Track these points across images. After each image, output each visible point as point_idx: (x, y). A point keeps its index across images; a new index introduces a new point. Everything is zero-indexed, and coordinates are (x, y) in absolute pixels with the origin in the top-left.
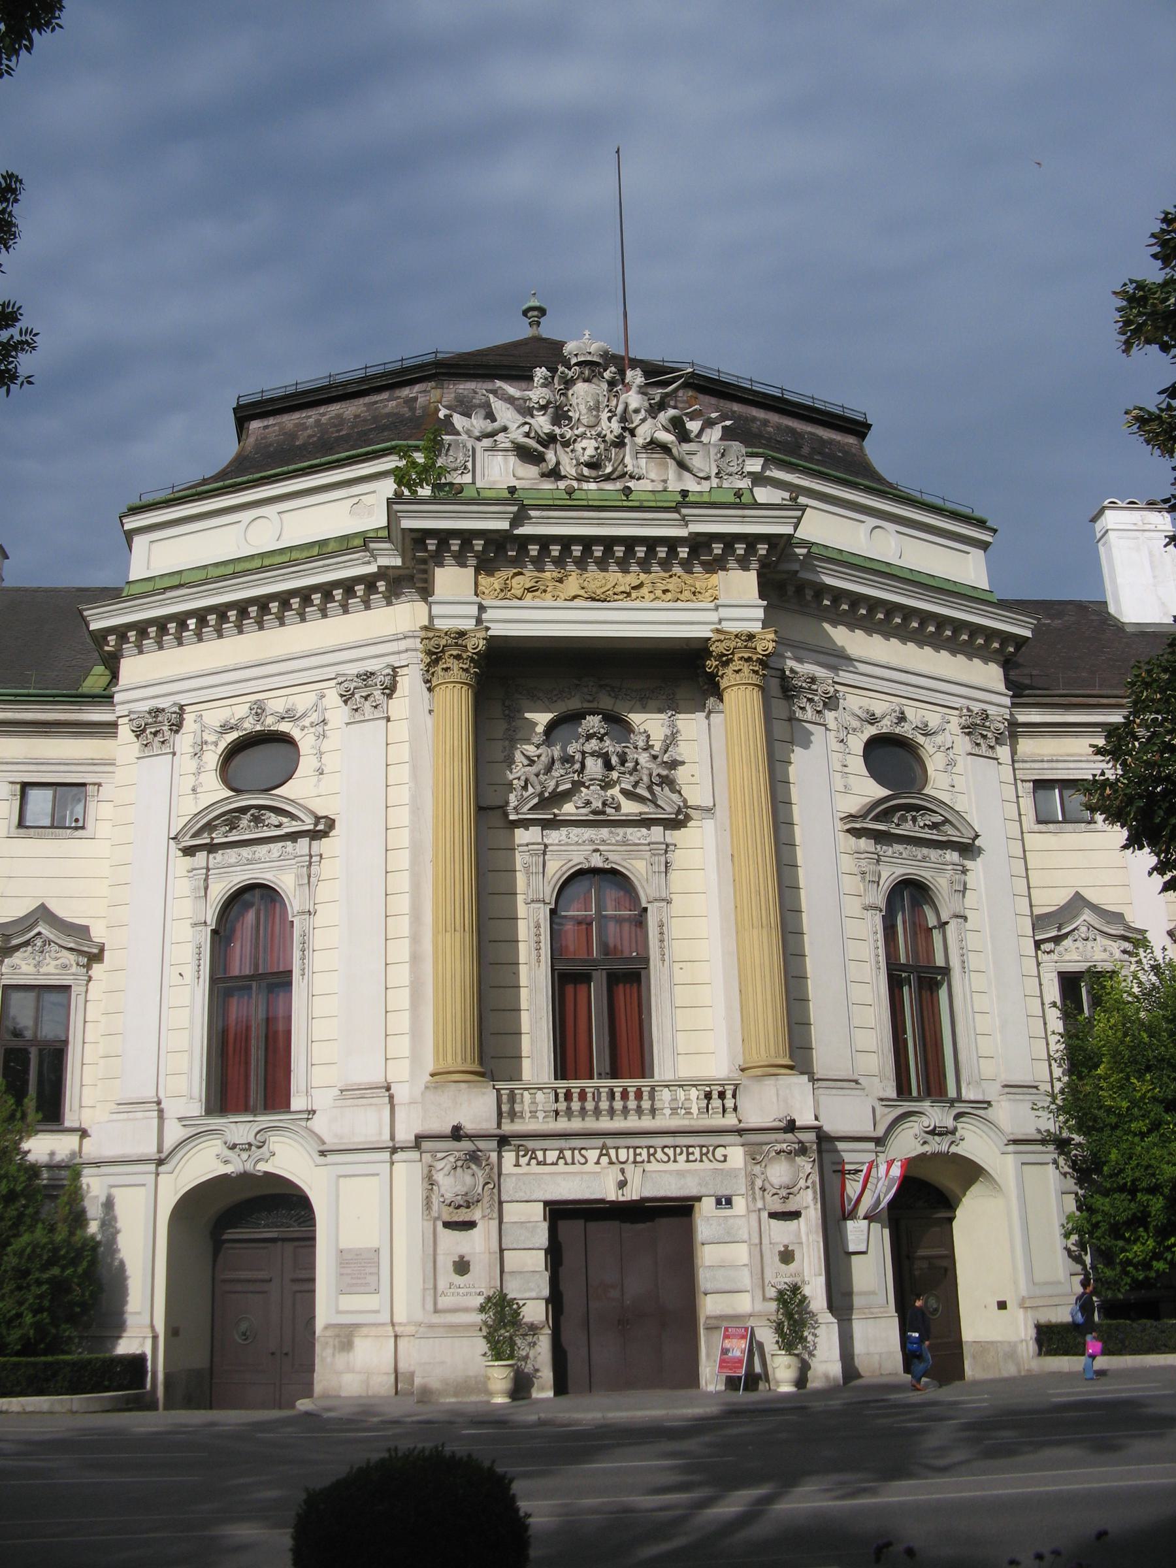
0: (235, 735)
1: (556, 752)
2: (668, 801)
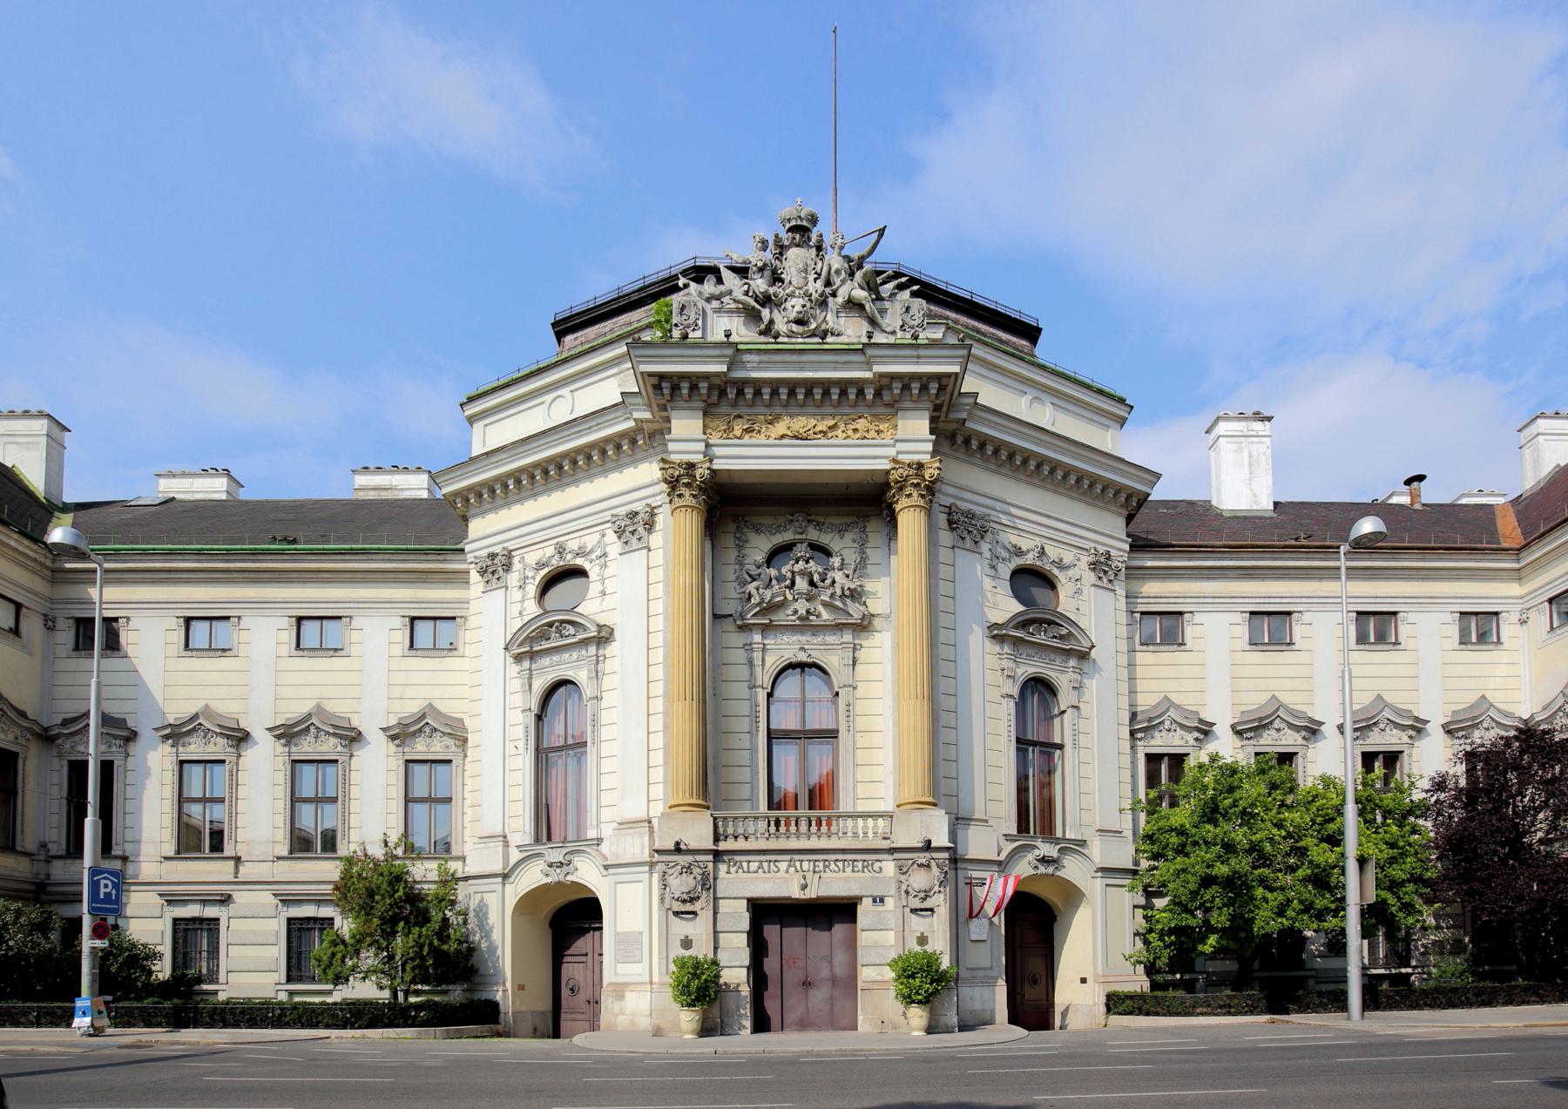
1: (773, 572)
2: (855, 610)
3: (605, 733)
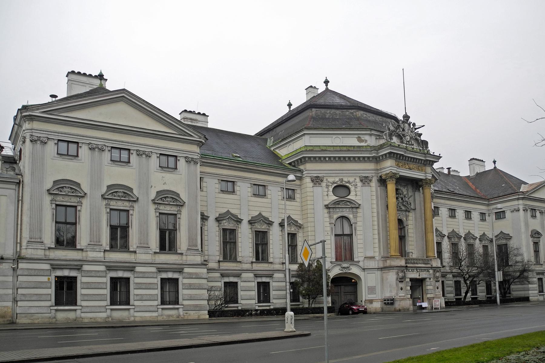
0: (336, 185)
3: (358, 233)
